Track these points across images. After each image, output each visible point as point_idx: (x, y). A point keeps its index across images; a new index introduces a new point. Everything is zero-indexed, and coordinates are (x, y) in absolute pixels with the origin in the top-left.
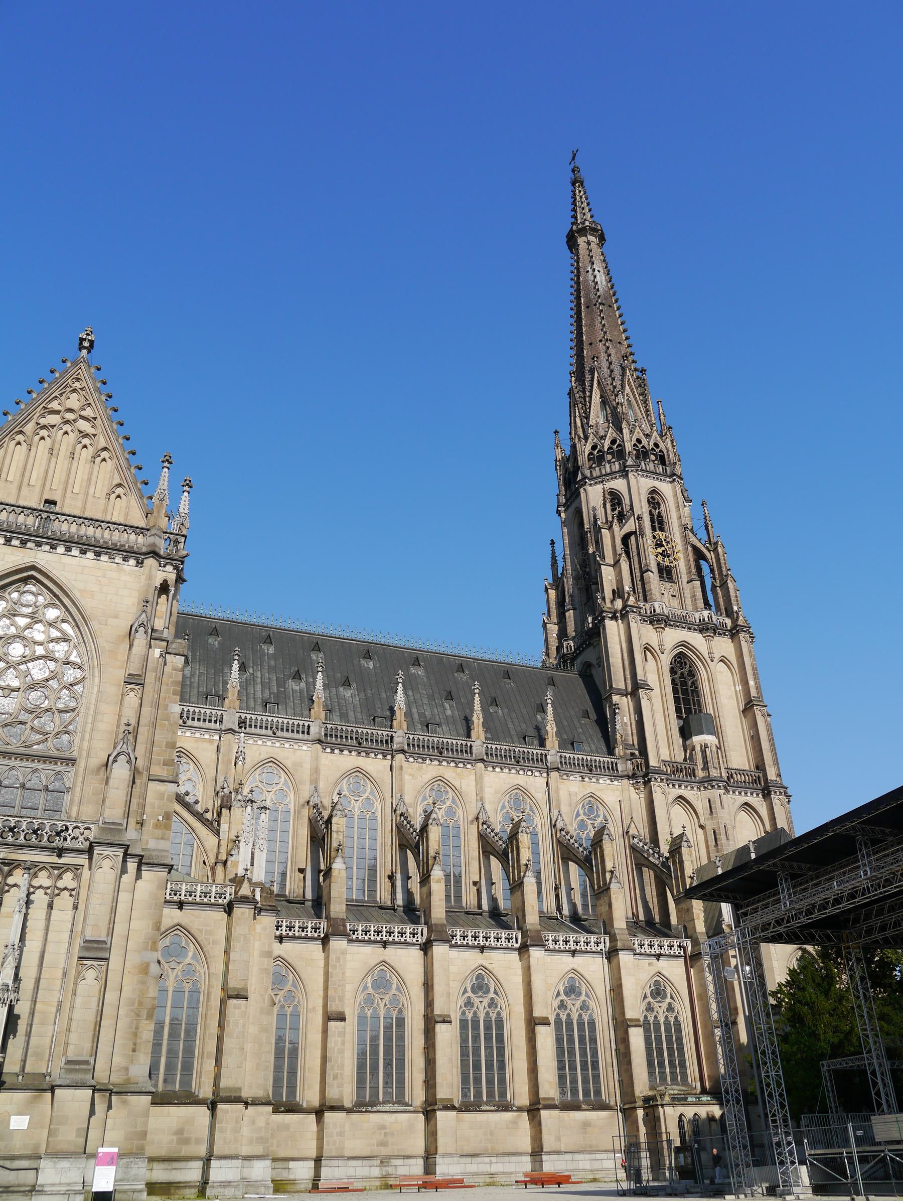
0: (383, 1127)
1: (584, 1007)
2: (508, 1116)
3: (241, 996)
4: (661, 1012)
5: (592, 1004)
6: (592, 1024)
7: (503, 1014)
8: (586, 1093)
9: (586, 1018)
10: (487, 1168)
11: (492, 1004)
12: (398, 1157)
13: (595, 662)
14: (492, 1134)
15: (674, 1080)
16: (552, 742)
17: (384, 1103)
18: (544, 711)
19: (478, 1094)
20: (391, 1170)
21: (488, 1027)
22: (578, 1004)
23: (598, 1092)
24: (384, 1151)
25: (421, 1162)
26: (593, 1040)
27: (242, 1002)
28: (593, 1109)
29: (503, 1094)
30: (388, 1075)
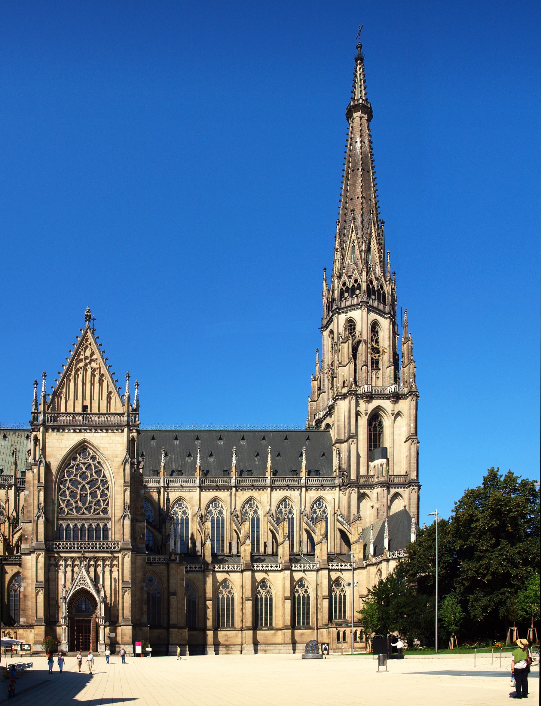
0: (226, 635)
1: (306, 591)
2: (273, 632)
3: (174, 594)
4: (338, 592)
5: (309, 590)
6: (308, 598)
7: (273, 596)
8: (303, 623)
9: (306, 596)
10: (264, 648)
11: (268, 592)
12: (232, 645)
13: (331, 424)
14: (266, 637)
15: (340, 618)
16: (303, 474)
17: (227, 627)
18: (301, 455)
19: (261, 624)
20: (229, 649)
21: (266, 601)
22: (303, 590)
23: (308, 623)
24: (227, 643)
25: (240, 646)
26: (308, 604)
27: (175, 597)
28: (305, 629)
29: (271, 624)
30: (228, 618)
